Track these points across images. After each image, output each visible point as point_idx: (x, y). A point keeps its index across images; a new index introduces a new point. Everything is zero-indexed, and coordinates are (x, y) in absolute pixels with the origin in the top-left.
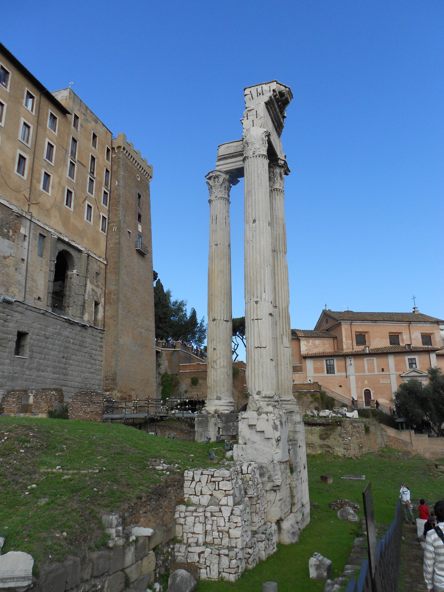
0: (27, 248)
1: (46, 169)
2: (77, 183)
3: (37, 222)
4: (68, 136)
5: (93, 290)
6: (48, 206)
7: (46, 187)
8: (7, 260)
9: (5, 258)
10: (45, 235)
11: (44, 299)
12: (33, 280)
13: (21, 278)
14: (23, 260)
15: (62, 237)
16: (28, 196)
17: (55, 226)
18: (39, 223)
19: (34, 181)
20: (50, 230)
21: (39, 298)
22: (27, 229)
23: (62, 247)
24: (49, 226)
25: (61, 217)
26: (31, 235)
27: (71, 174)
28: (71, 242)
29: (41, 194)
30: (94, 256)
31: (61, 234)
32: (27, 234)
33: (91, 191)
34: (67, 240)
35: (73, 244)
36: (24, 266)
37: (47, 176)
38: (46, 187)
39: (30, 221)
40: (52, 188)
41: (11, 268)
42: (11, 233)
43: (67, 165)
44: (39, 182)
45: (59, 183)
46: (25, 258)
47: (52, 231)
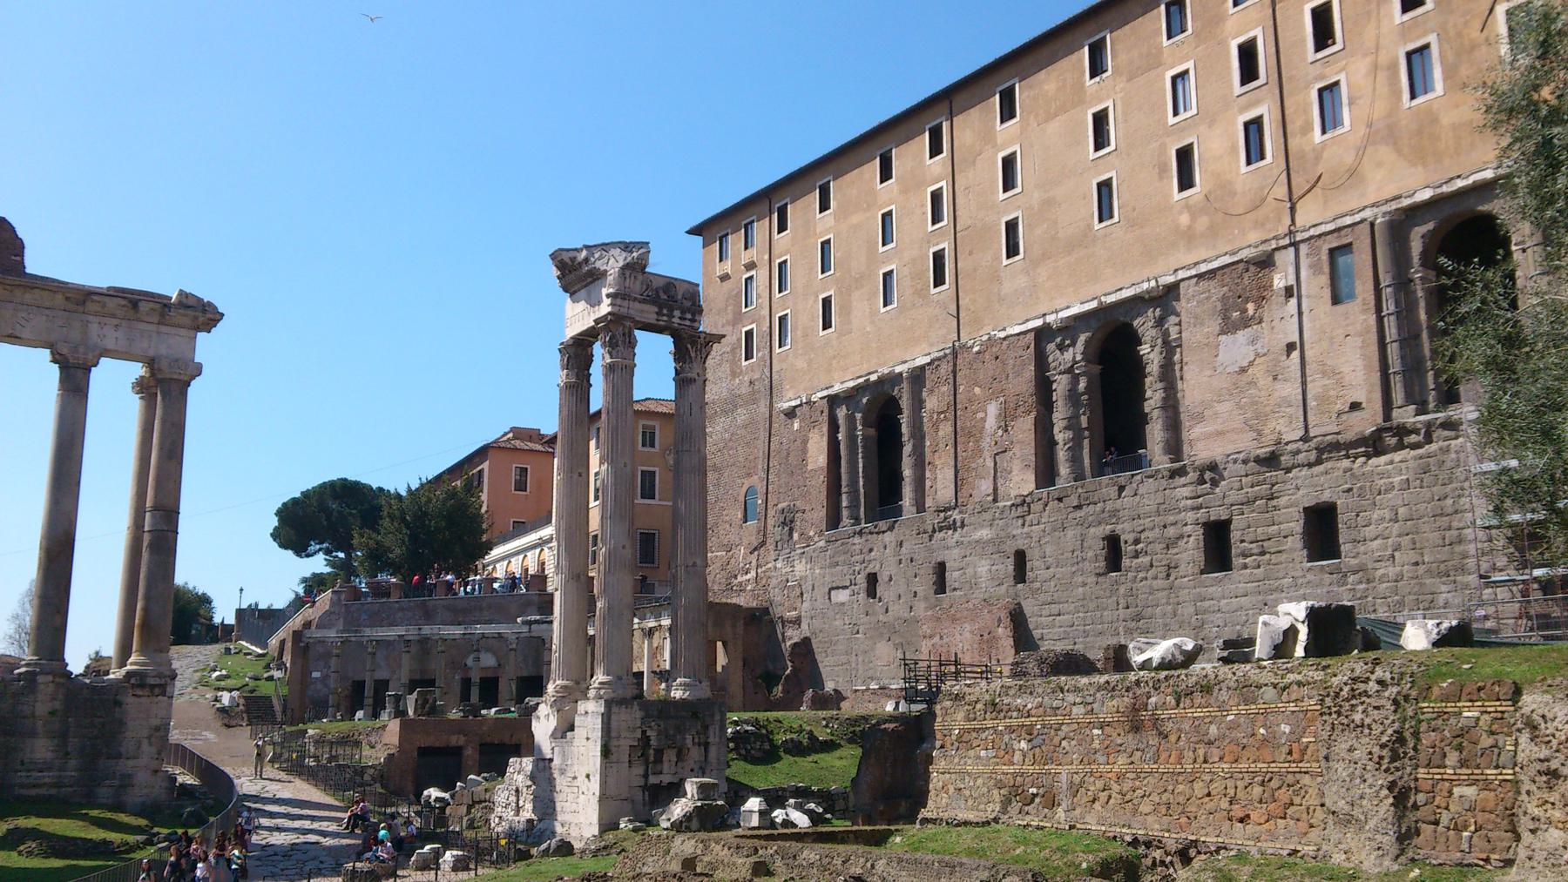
0: (1295, 311)
6: (1349, 159)
7: (1329, 120)
9: (1243, 370)
10: (1345, 241)
11: (1369, 401)
13: (1291, 390)
14: (1290, 347)
15: (1406, 202)
16: (1281, 191)
20: (1357, 218)
21: (1355, 406)
22: (1291, 270)
24: (1352, 213)
25: (1398, 151)
28: (1446, 189)
29: (1318, 152)
32: (1292, 281)
34: (1425, 195)
35: (1460, 184)
37: (1328, 92)
38: (1329, 120)
39: (1295, 245)
40: (1350, 104)
41: (1261, 383)
42: (1251, 307)
44: (1308, 128)
45: (1375, 67)
46: (1295, 338)
47: (1367, 214)
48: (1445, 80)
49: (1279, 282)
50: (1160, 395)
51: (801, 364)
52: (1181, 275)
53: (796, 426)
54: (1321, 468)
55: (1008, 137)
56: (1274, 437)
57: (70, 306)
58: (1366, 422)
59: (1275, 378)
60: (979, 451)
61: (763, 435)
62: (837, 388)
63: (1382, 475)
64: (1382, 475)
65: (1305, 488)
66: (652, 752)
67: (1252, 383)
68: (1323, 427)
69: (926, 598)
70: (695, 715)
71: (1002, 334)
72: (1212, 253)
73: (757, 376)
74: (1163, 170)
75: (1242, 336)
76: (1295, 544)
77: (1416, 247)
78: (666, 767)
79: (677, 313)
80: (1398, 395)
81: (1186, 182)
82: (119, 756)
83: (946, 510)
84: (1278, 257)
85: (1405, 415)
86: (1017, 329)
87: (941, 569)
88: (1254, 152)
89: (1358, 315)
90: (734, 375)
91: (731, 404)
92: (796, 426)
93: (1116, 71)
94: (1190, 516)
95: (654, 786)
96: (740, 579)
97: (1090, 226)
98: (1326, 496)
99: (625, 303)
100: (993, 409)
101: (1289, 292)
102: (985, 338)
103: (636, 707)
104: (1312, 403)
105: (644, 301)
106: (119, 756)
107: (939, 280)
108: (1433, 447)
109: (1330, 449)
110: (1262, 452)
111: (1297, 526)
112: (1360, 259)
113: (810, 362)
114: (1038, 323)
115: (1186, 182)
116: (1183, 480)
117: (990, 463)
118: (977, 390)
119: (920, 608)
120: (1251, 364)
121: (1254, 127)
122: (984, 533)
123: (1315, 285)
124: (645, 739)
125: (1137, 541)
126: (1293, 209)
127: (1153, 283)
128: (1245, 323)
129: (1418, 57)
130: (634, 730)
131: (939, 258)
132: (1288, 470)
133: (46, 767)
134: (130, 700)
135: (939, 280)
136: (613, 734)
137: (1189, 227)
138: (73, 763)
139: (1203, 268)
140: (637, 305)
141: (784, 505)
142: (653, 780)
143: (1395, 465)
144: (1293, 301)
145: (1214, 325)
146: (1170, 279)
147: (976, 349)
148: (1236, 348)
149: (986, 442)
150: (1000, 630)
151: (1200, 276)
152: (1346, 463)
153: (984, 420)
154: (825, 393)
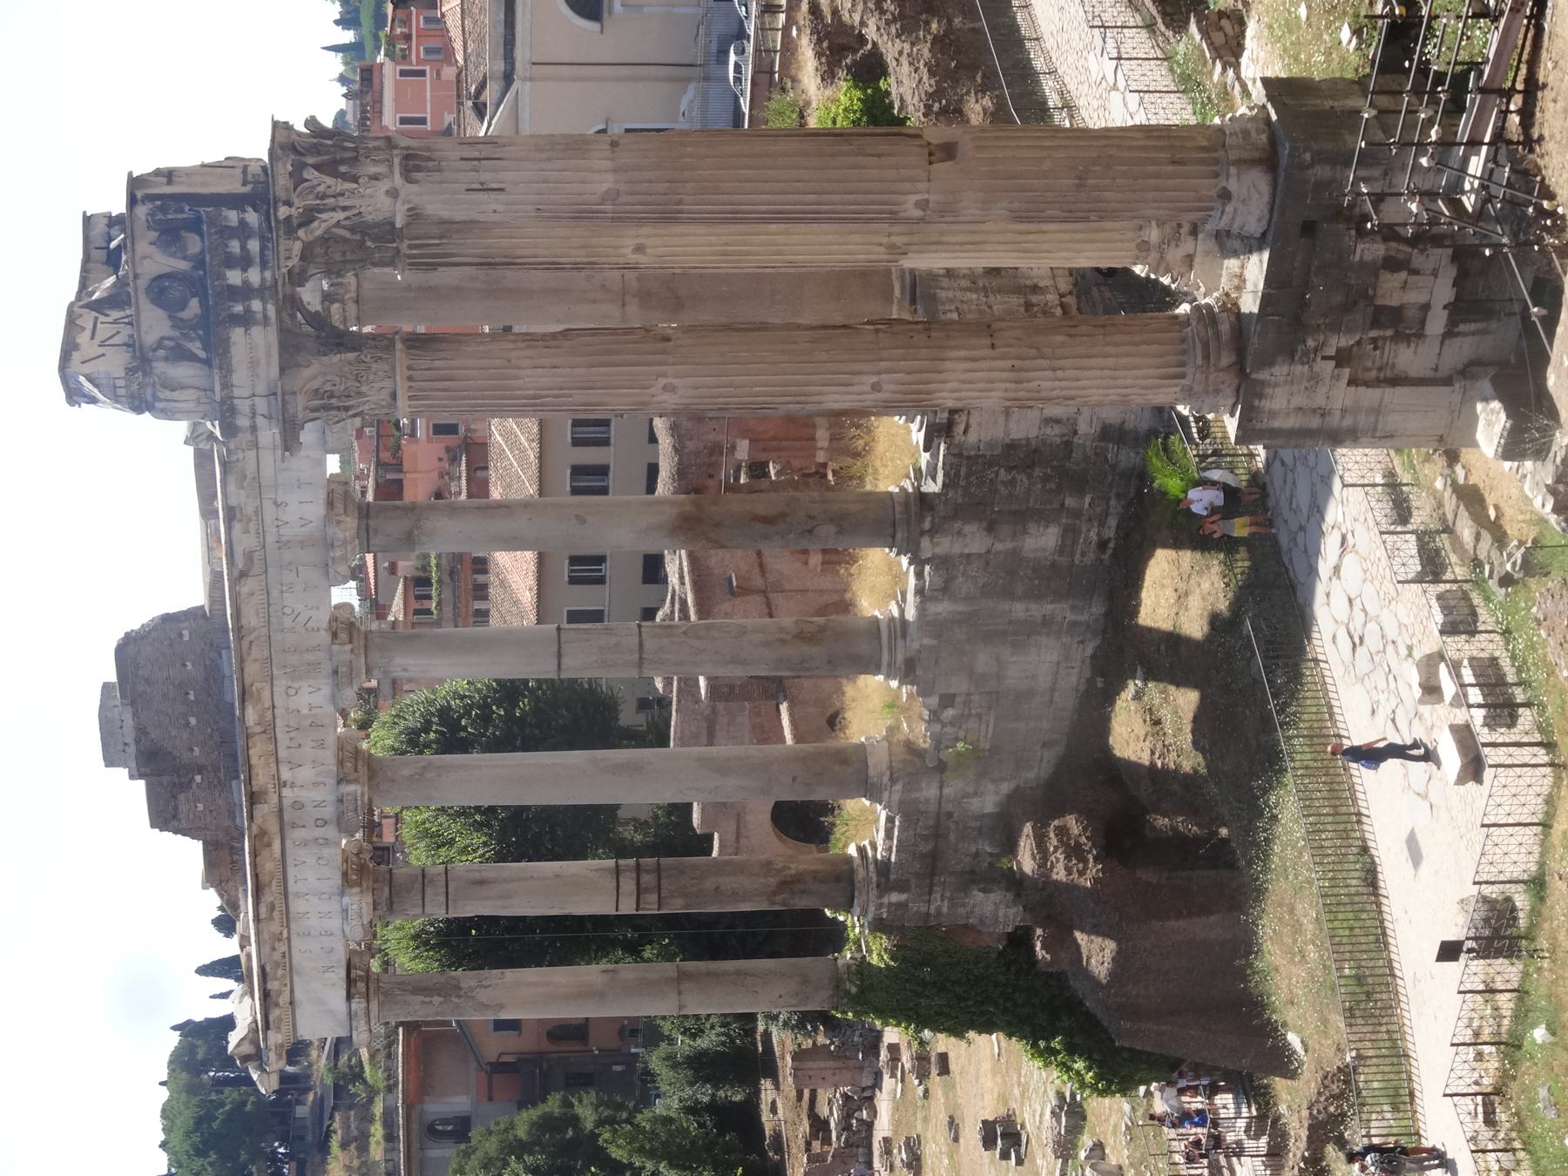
57: (256, 569)
66: (1373, 334)
70: (1309, 228)
78: (1414, 297)
79: (234, 277)
82: (1068, 445)
95: (1452, 322)
99: (243, 406)
103: (1263, 375)
105: (227, 370)
106: (1068, 445)
124: (1342, 358)
130: (1315, 379)
133: (1070, 533)
134: (972, 437)
136: (1315, 422)
138: (1070, 502)
140: (240, 377)
142: (1437, 323)
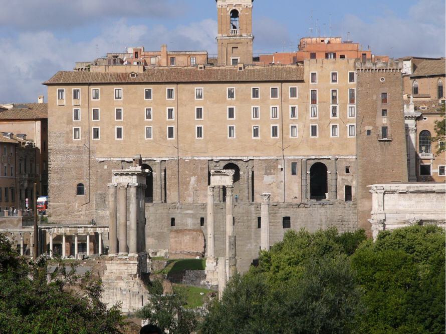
1: (292, 124)
2: (320, 119)
3: (289, 158)
4: (308, 91)
5: (343, 179)
8: (272, 185)
9: (270, 184)
12: (289, 189)
13: (282, 191)
15: (309, 158)
17: (307, 153)
18: (290, 158)
19: (284, 136)
20: (299, 158)
23: (313, 162)
26: (286, 166)
27: (315, 116)
30: (342, 157)
31: (308, 156)
32: (283, 167)
33: (334, 114)
34: (314, 158)
35: (320, 157)
36: (283, 184)
40: (299, 132)
41: (274, 188)
42: (272, 171)
43: (309, 111)
44: (288, 134)
47: (301, 157)
48: (319, 134)
49: (280, 167)
50: (246, 186)
51: (105, 146)
52: (254, 158)
53: (106, 167)
54: (287, 209)
55: (198, 103)
56: (277, 201)
58: (298, 201)
59: (278, 188)
60: (187, 189)
61: (86, 167)
62: (126, 159)
63: (300, 213)
64: (300, 213)
65: (283, 213)
67: (272, 188)
68: (289, 200)
69: (167, 227)
71: (197, 158)
72: (262, 155)
73: (81, 145)
74: (250, 130)
75: (270, 177)
76: (281, 223)
77: (309, 167)
80: (304, 197)
81: (256, 134)
83: (175, 203)
84: (279, 161)
85: (305, 201)
86: (202, 158)
87: (173, 220)
88: (275, 134)
89: (297, 178)
90: (68, 142)
91: (67, 152)
92: (106, 167)
93: (237, 100)
94: (254, 215)
96: (76, 213)
97: (227, 138)
98: (288, 215)
100: (193, 179)
101: (282, 169)
102: (190, 158)
104: (286, 195)
107: (171, 135)
108: (311, 209)
109: (290, 205)
110: (275, 204)
111: (281, 220)
112: (298, 167)
113: (110, 147)
114: (211, 159)
115: (256, 134)
116: (253, 206)
117: (192, 193)
118: (187, 172)
119: (166, 230)
120: (272, 183)
121: (275, 129)
122: (190, 212)
123: (288, 170)
125: (239, 219)
126: (283, 150)
127: (246, 158)
128: (271, 174)
129: (314, 129)
131: (171, 130)
132: (279, 208)
135: (171, 135)
137: (256, 147)
139: (261, 158)
141: (100, 192)
143: (302, 210)
144: (283, 172)
145: (264, 172)
146: (252, 158)
147: (186, 161)
148: (268, 179)
149: (191, 187)
150: (200, 238)
151: (260, 159)
152: (292, 209)
153: (190, 180)
154: (121, 159)
